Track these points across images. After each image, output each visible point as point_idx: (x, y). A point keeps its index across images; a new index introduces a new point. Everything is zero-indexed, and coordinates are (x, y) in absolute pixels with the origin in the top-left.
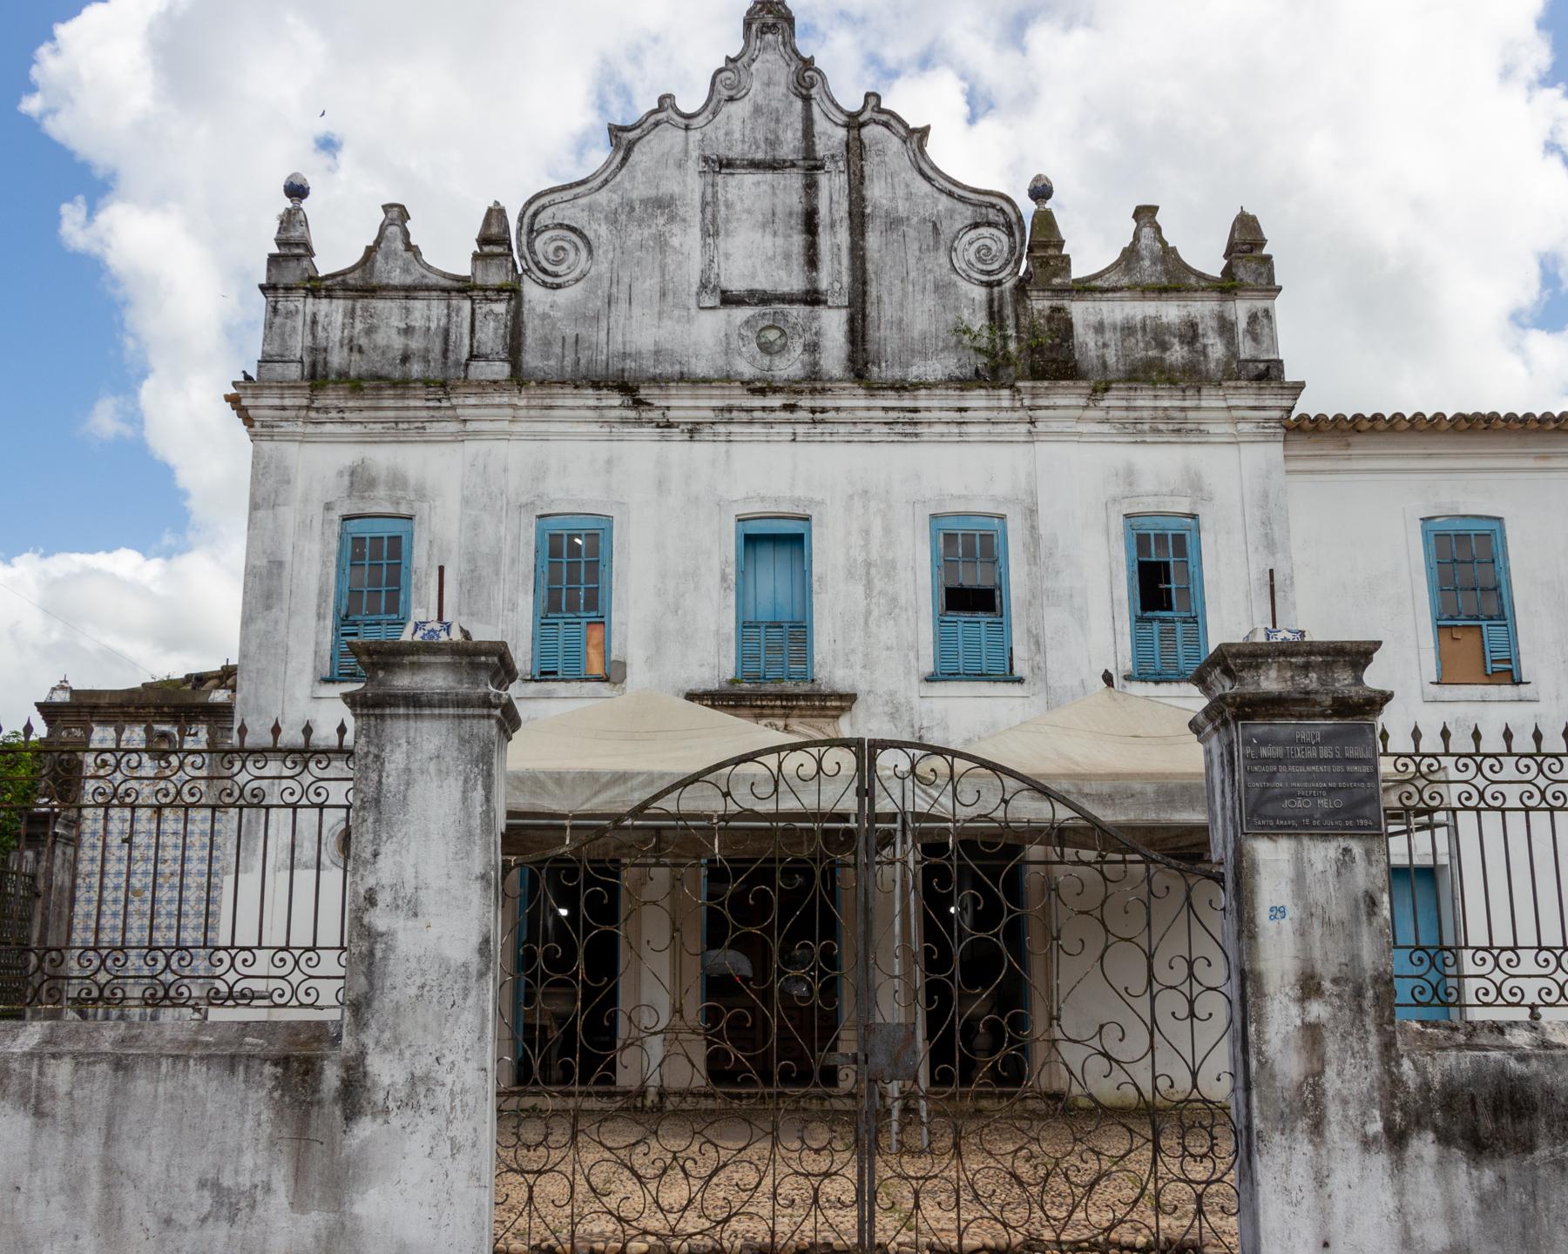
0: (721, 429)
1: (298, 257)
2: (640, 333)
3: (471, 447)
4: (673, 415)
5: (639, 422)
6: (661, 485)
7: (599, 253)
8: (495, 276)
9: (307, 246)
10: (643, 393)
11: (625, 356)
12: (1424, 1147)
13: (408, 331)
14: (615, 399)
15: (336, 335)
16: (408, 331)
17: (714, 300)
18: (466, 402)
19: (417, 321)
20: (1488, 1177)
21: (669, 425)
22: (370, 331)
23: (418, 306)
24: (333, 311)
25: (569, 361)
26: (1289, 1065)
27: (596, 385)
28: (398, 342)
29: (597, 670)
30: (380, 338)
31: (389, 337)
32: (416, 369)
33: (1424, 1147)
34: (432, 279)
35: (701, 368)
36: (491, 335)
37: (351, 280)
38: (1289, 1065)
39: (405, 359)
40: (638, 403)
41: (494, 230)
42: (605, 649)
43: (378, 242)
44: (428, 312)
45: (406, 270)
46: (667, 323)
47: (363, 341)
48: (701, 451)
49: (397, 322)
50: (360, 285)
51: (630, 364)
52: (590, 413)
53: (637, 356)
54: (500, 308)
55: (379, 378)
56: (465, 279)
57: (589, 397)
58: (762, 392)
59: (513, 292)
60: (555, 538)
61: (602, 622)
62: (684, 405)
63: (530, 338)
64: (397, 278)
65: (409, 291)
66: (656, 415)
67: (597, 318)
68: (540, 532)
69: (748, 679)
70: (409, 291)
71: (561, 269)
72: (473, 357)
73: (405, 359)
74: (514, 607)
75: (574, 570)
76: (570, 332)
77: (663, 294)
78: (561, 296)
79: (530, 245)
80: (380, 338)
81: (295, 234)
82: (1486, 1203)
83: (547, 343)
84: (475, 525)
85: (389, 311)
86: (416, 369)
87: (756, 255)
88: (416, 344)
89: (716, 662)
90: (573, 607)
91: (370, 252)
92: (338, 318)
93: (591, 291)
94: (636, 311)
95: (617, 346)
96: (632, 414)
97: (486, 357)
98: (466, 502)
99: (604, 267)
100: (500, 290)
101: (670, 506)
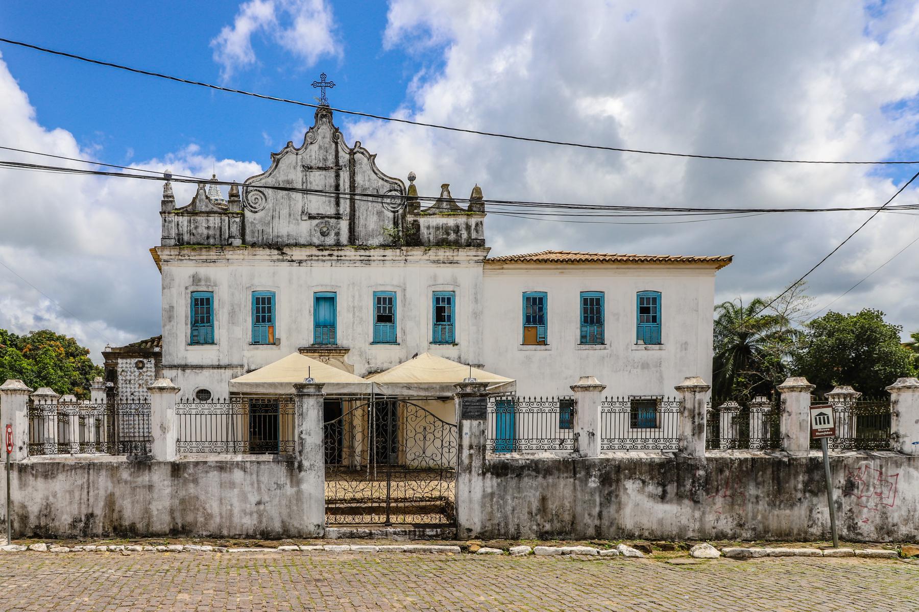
0: (309, 262)
1: (171, 202)
2: (283, 228)
3: (231, 268)
4: (294, 258)
5: (283, 261)
6: (290, 281)
7: (269, 200)
8: (235, 209)
9: (172, 196)
10: (285, 250)
11: (278, 237)
12: (489, 475)
13: (208, 228)
14: (276, 252)
15: (185, 229)
16: (208, 228)
17: (306, 218)
18: (229, 254)
19: (212, 225)
20: (499, 480)
21: (292, 261)
22: (196, 228)
23: (211, 219)
24: (184, 220)
25: (260, 238)
26: (466, 461)
27: (270, 248)
28: (205, 232)
29: (271, 341)
30: (200, 230)
31: (202, 230)
32: (212, 241)
33: (489, 475)
34: (215, 209)
35: (302, 241)
36: (235, 229)
37: (189, 209)
38: (466, 461)
39: (208, 237)
40: (283, 253)
41: (235, 192)
42: (273, 334)
43: (197, 196)
44: (214, 221)
45: (207, 206)
46: (291, 225)
47: (194, 231)
48: (303, 269)
49: (204, 225)
50: (191, 211)
51: (280, 240)
52: (268, 258)
53: (282, 237)
54: (238, 220)
55: (199, 244)
56: (226, 210)
57: (267, 251)
58: (322, 250)
59: (243, 215)
60: (258, 299)
61: (273, 327)
62: (298, 254)
63: (248, 231)
64: (204, 209)
65: (208, 213)
66: (288, 258)
67: (269, 223)
68: (253, 296)
69: (318, 344)
70: (208, 213)
71: (256, 206)
72: (230, 237)
73: (208, 237)
74: (246, 321)
75: (264, 309)
76: (260, 228)
77: (290, 215)
78: (257, 216)
79: (247, 197)
80: (200, 230)
81: (169, 192)
82: (498, 485)
83: (253, 232)
84: (233, 294)
85: (201, 219)
86: (212, 241)
87: (320, 205)
88: (211, 232)
89: (308, 339)
90: (264, 321)
91: (194, 199)
92: (186, 223)
93: (267, 215)
94: (281, 221)
95: (275, 233)
96: (281, 257)
97: (234, 237)
98: (230, 287)
99: (271, 205)
100: (238, 214)
101: (294, 287)
